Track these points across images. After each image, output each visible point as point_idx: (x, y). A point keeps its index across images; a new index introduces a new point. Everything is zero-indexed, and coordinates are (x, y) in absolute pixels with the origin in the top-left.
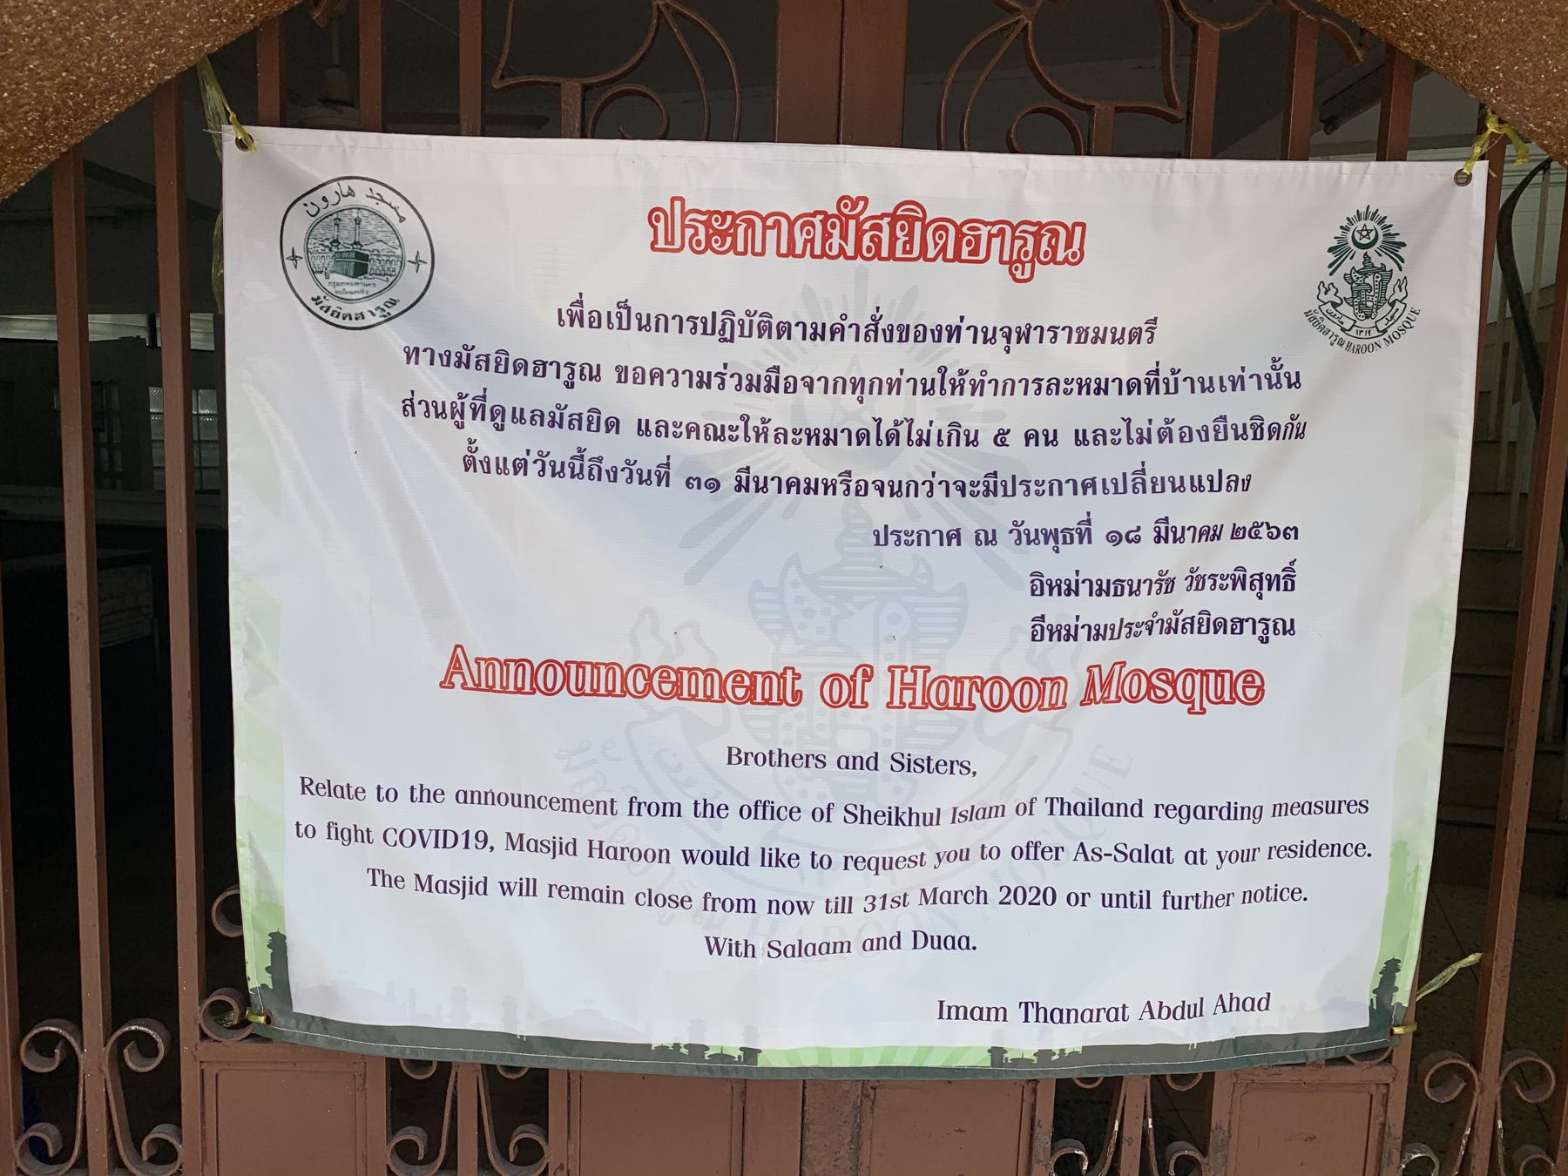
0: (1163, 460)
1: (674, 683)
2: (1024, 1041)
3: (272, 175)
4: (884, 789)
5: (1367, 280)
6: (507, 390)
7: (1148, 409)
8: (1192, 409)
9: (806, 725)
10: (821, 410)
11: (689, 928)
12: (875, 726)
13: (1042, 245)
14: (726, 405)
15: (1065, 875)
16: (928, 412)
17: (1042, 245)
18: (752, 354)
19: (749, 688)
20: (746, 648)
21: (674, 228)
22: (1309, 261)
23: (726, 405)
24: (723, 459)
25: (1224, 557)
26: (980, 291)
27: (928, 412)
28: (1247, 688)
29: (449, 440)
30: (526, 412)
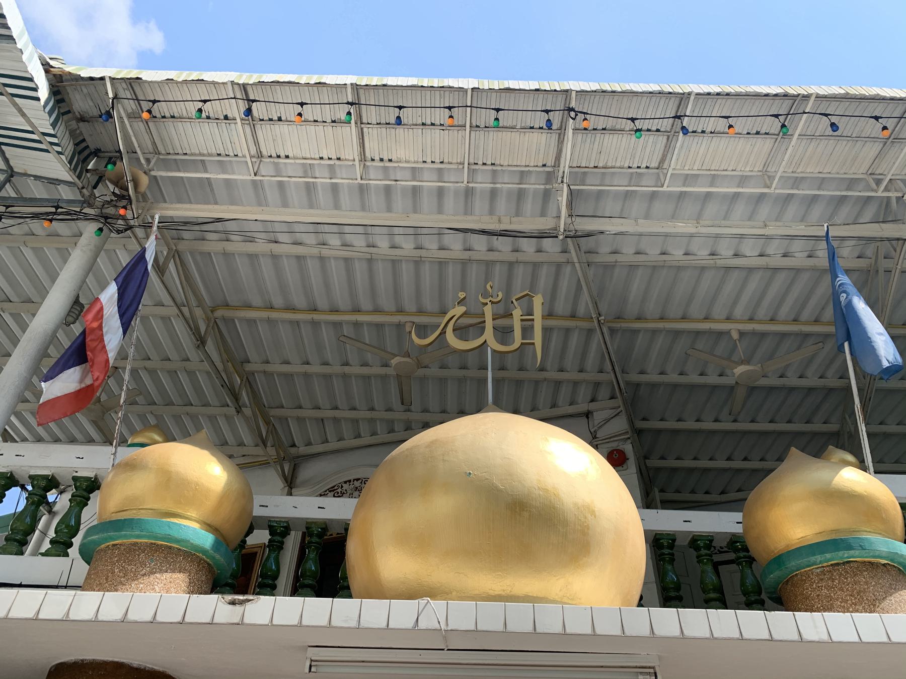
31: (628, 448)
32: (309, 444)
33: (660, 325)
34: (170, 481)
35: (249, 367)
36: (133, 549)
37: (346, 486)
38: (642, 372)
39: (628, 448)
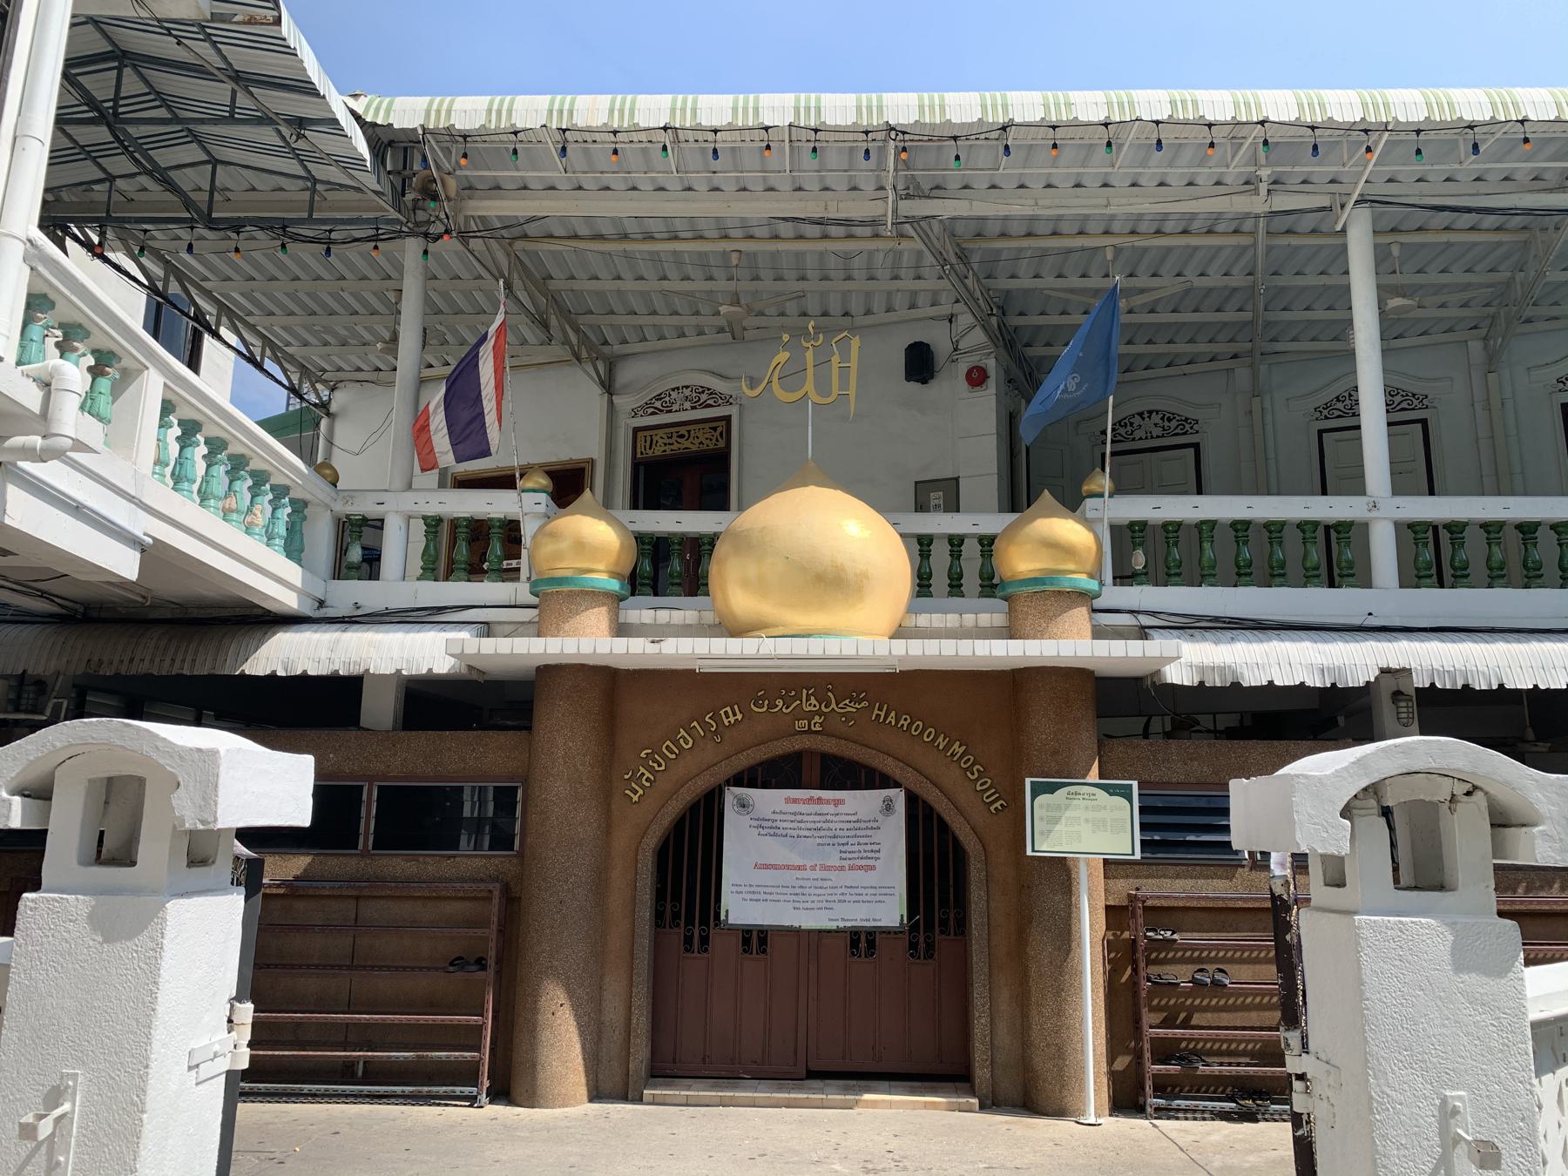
0: (859, 833)
1: (788, 867)
2: (841, 925)
3: (732, 794)
4: (820, 883)
5: (888, 807)
6: (765, 824)
7: (857, 825)
8: (863, 825)
9: (808, 874)
10: (809, 825)
11: (791, 905)
12: (818, 874)
13: (838, 802)
14: (795, 825)
15: (847, 898)
16: (825, 826)
17: (838, 802)
18: (799, 818)
19: (799, 868)
20: (798, 861)
21: (788, 800)
22: (879, 803)
23: (795, 825)
24: (795, 833)
25: (869, 847)
26: (830, 808)
27: (825, 826)
28: (873, 868)
29: (756, 831)
30: (767, 827)
31: (991, 364)
32: (624, 342)
33: (1025, 243)
34: (581, 546)
35: (553, 285)
36: (571, 594)
37: (674, 395)
38: (1012, 277)
39: (991, 364)
